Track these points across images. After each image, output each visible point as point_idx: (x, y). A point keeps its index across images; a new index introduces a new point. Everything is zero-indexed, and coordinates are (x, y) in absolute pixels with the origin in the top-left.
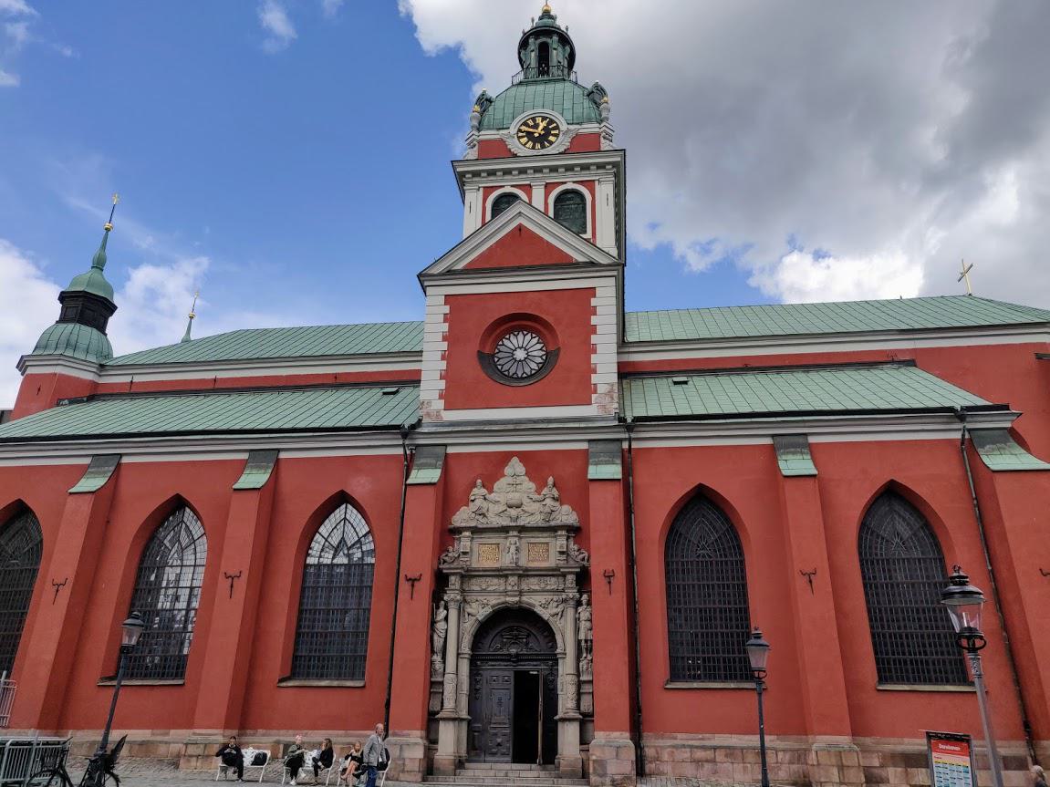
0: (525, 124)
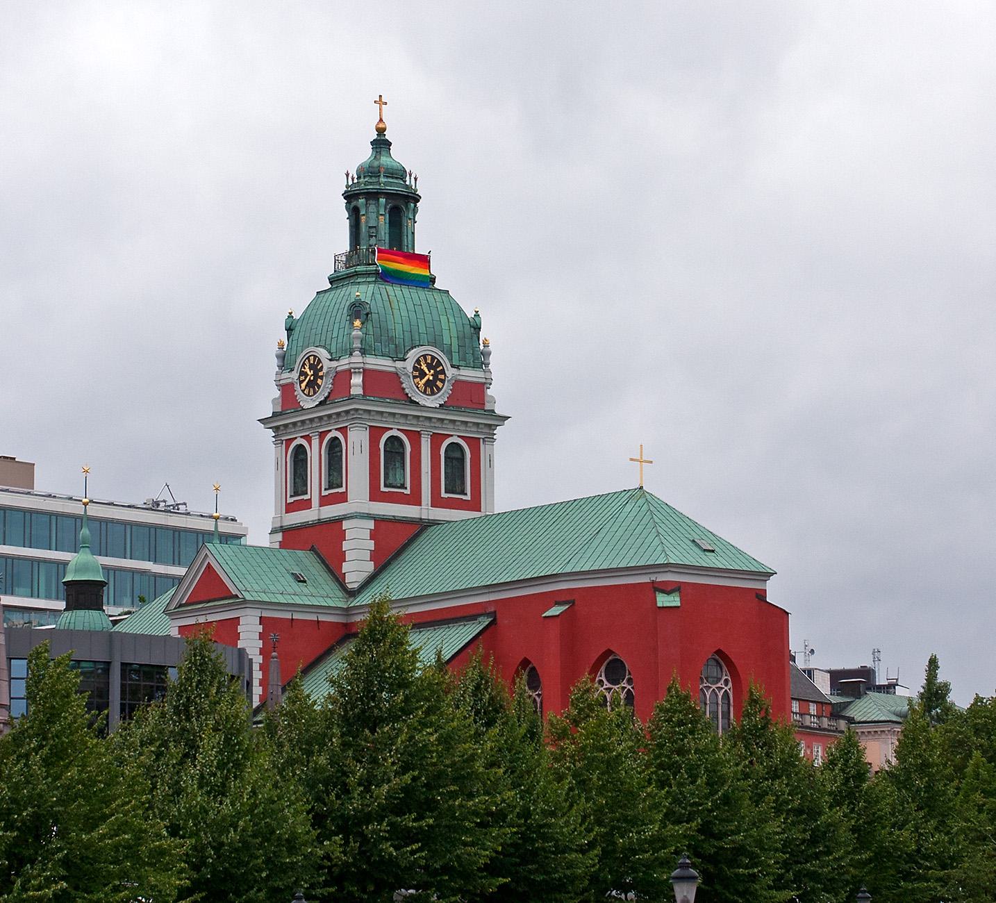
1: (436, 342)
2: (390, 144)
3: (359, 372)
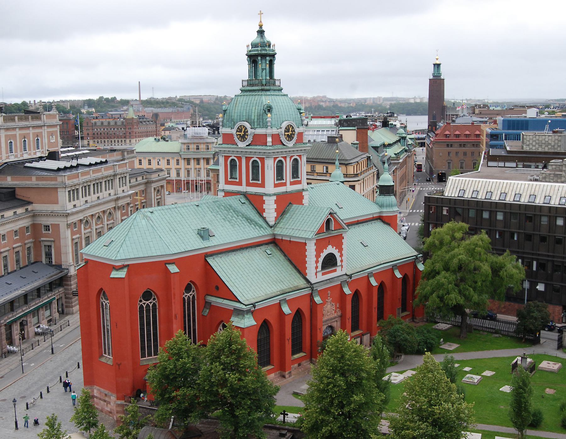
0: (238, 128)
2: (264, 32)
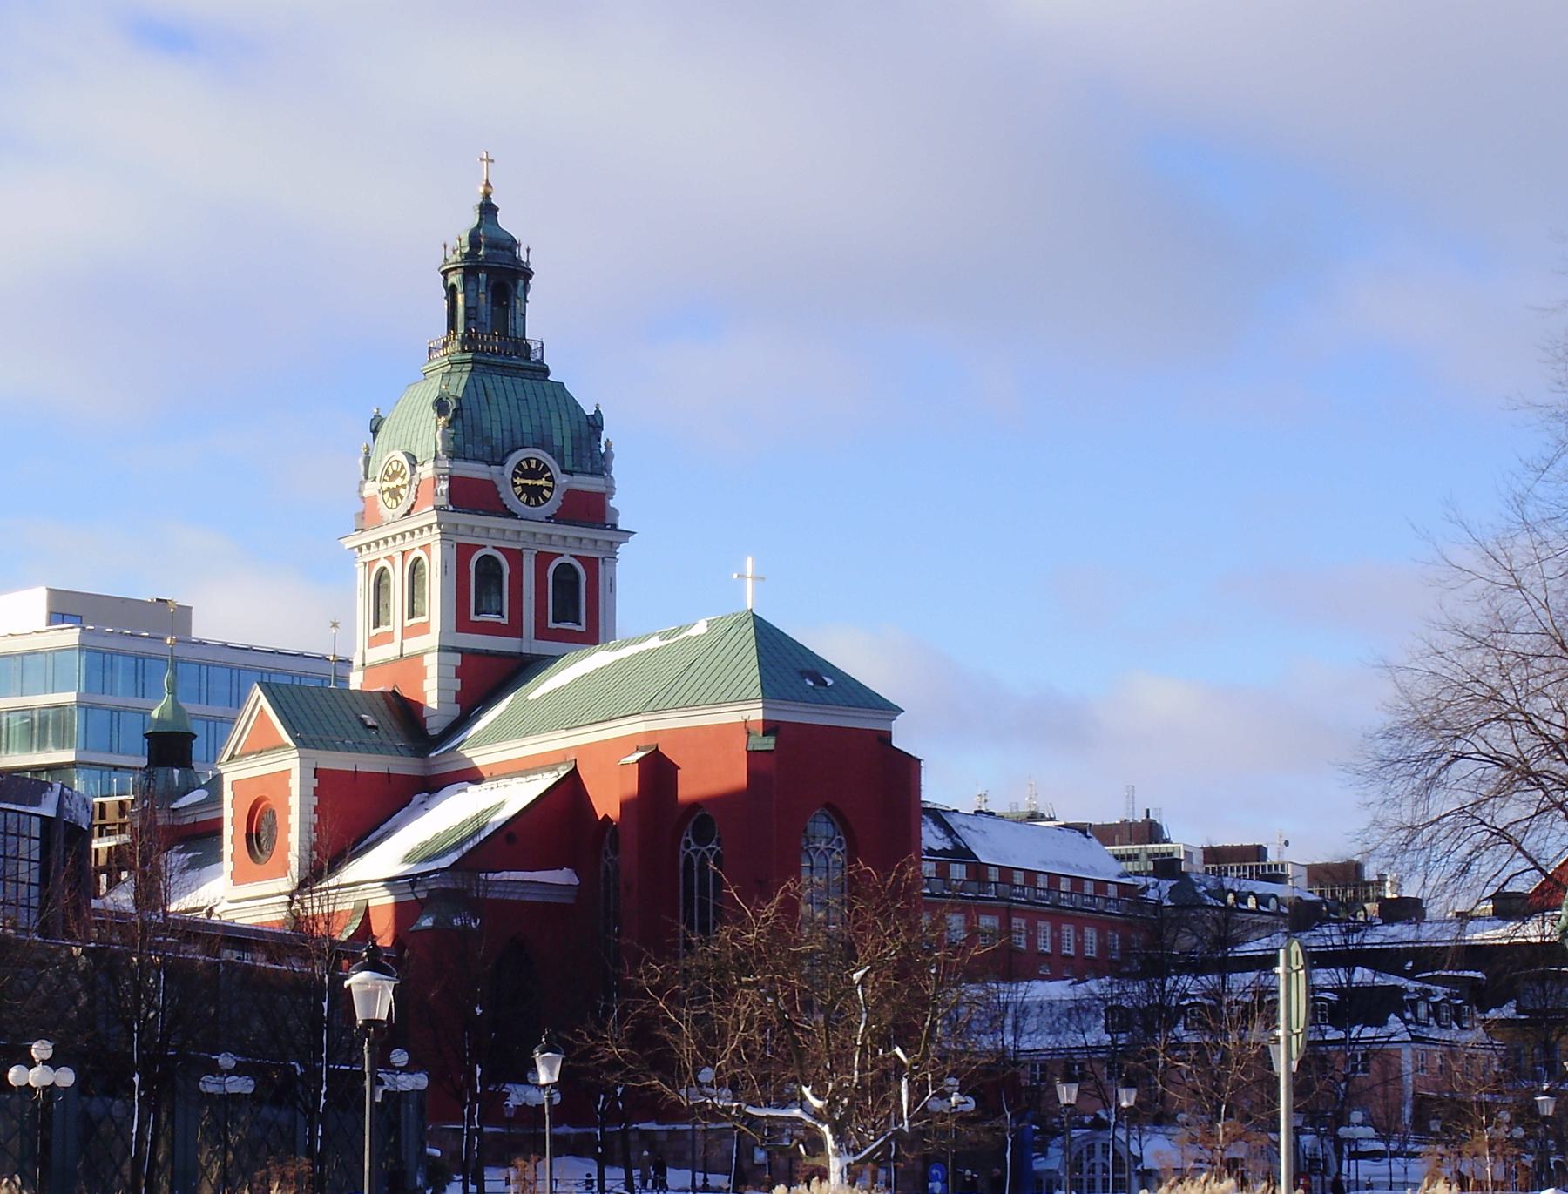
0: (519, 466)
1: (542, 445)
3: (445, 480)
